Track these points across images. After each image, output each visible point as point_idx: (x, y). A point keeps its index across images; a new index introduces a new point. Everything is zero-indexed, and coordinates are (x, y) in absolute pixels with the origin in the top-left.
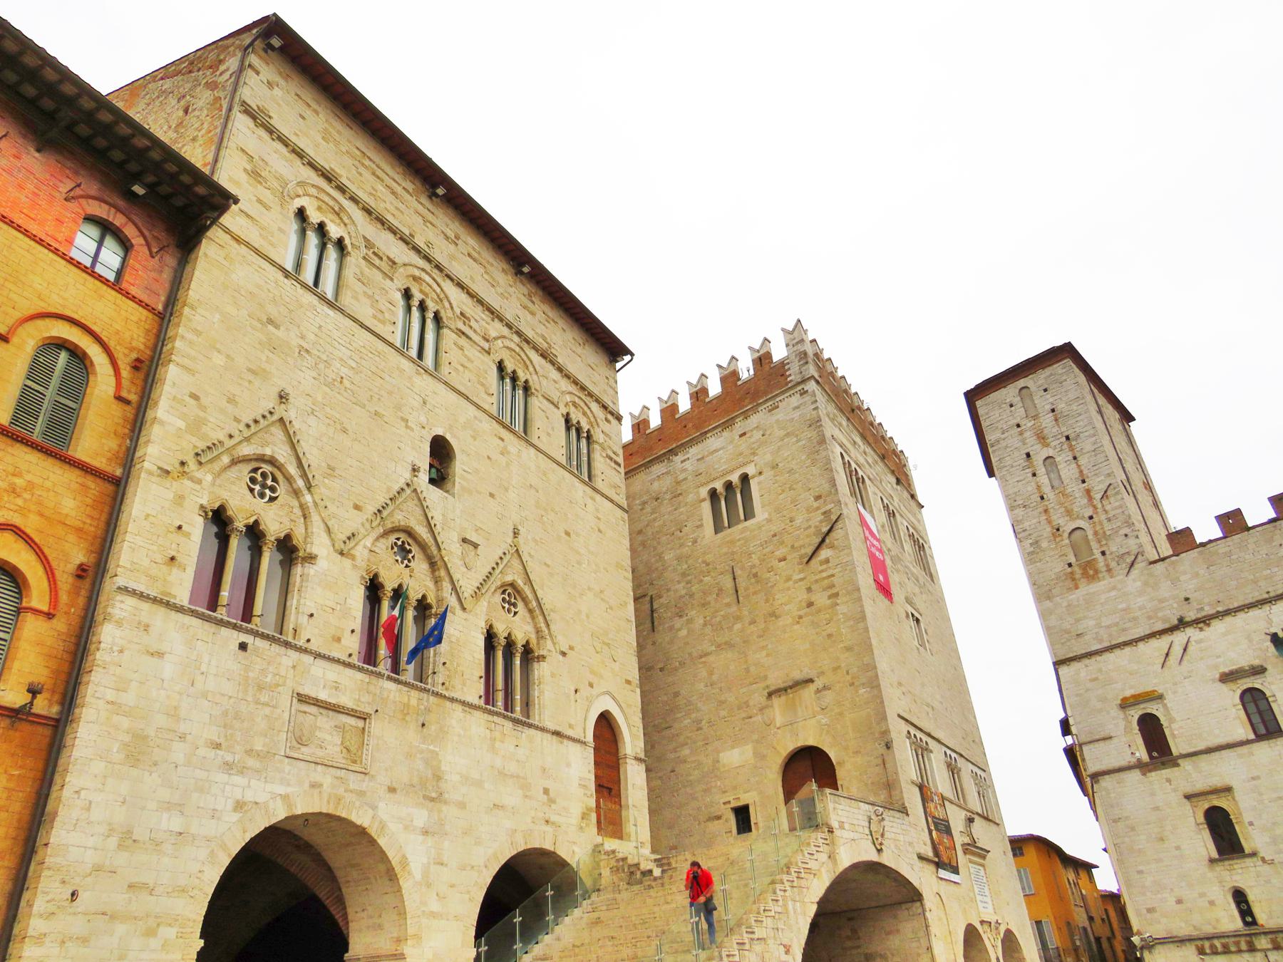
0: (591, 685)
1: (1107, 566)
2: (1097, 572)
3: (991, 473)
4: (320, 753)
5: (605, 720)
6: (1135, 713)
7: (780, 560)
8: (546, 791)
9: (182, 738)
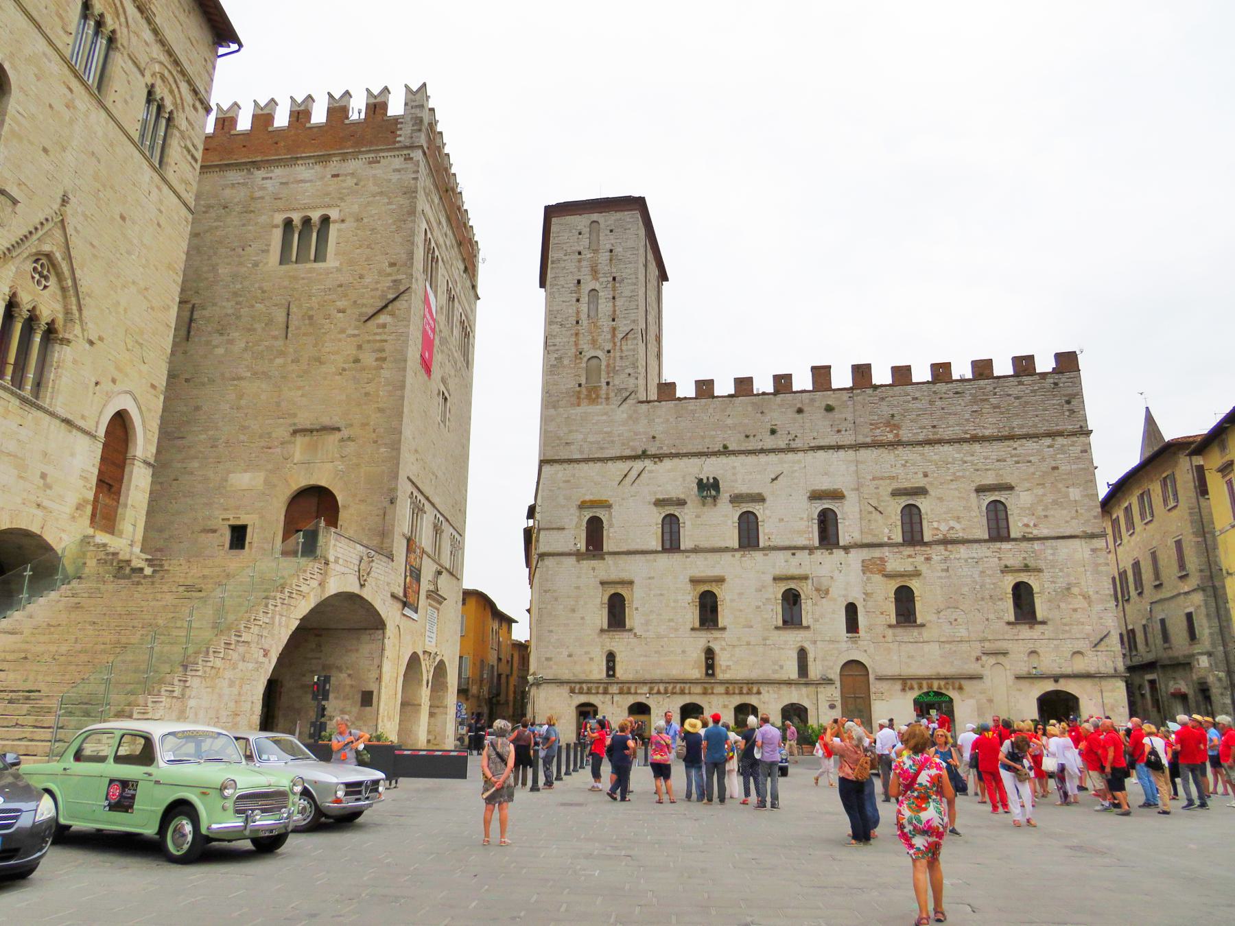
0: (114, 381)
1: (607, 394)
2: (598, 397)
3: (543, 284)
5: (121, 421)
6: (588, 515)
7: (339, 311)
8: (44, 476)
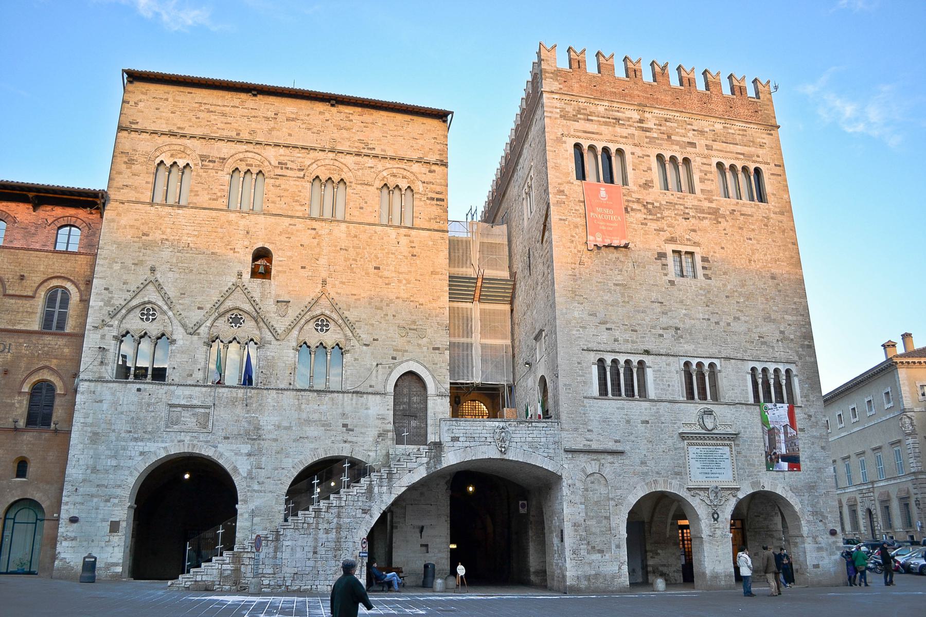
0: (394, 358)
4: (184, 427)
8: (345, 425)
9: (114, 431)
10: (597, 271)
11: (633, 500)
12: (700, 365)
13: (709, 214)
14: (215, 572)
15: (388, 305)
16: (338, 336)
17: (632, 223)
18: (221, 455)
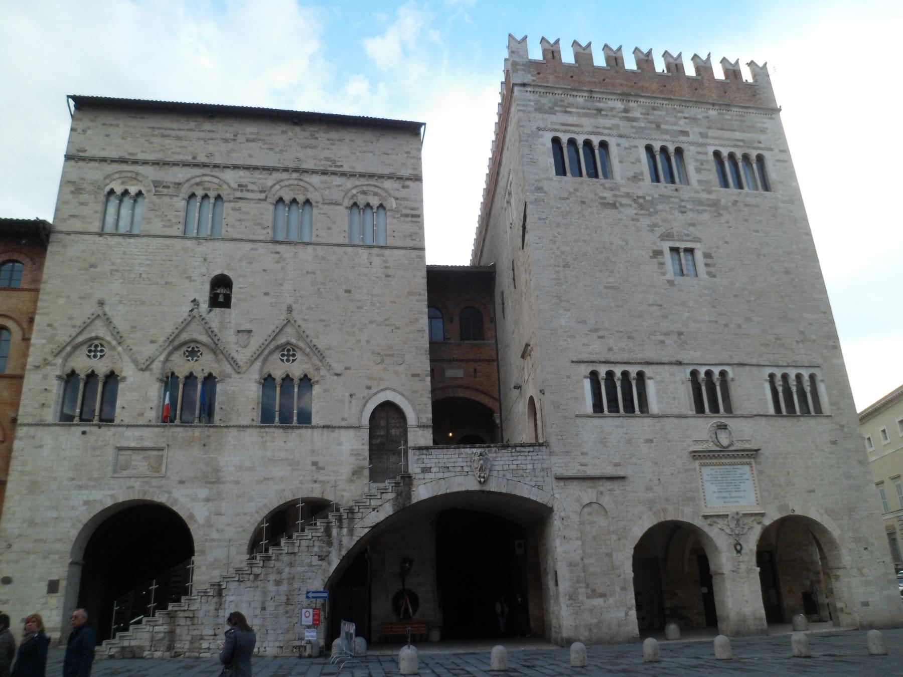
0: (369, 388)
4: (134, 472)
8: (315, 464)
9: (55, 479)
10: (585, 273)
11: (638, 532)
12: (709, 374)
13: (709, 206)
14: (146, 636)
15: (361, 330)
16: (307, 366)
17: (621, 219)
18: (175, 501)
